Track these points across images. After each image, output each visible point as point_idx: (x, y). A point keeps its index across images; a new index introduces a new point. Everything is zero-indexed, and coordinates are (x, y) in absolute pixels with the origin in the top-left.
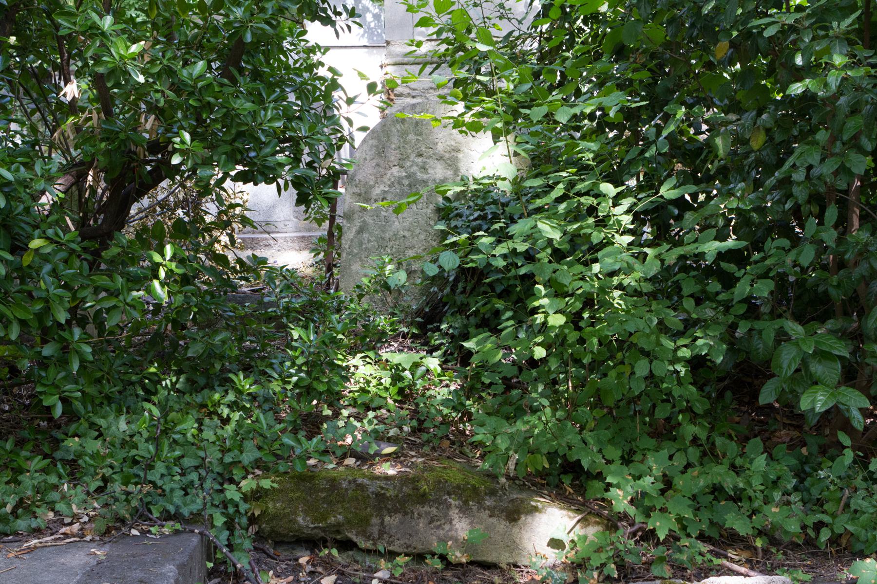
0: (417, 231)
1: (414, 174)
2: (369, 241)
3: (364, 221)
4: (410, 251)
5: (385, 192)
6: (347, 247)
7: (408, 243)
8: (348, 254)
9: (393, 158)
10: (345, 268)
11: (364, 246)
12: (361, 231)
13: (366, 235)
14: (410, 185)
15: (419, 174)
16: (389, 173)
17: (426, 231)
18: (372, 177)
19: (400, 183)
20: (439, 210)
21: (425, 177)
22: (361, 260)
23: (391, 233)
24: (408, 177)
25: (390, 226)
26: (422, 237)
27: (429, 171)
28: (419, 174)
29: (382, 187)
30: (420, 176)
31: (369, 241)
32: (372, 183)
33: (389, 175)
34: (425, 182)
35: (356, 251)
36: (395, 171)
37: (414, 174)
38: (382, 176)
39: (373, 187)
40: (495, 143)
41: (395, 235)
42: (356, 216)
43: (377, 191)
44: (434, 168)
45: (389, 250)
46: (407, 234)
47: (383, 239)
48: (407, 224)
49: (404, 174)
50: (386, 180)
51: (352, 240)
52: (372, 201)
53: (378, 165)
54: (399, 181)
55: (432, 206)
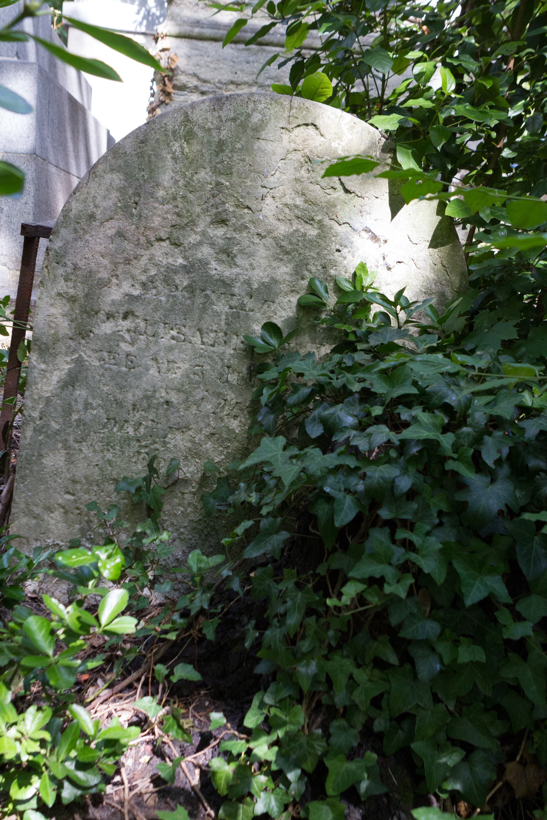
0: (199, 394)
1: (204, 263)
2: (87, 406)
3: (79, 361)
4: (179, 436)
5: (131, 298)
6: (36, 414)
7: (174, 419)
8: (38, 431)
9: (157, 221)
10: (29, 462)
11: (75, 417)
12: (71, 381)
13: (81, 393)
14: (191, 289)
15: (214, 264)
16: (146, 255)
17: (219, 395)
18: (105, 262)
19: (167, 281)
20: (250, 350)
21: (228, 272)
22: (66, 447)
23: (139, 393)
24: (187, 269)
25: (138, 377)
26: (209, 407)
27: (239, 260)
28: (214, 264)
29: (126, 287)
30: (217, 268)
31: (87, 406)
32: (104, 275)
33: (144, 261)
34: (225, 285)
35: (55, 426)
36: (162, 253)
37: (204, 263)
38: (127, 261)
39: (106, 283)
40: (394, 213)
41: (146, 397)
42: (61, 347)
43: (115, 294)
44: (250, 255)
45: (131, 431)
46: (174, 398)
47: (120, 404)
48: (176, 376)
49: (181, 261)
50: (137, 272)
51: (48, 401)
52: (102, 316)
53: (120, 234)
54: (168, 275)
55: (236, 341)
